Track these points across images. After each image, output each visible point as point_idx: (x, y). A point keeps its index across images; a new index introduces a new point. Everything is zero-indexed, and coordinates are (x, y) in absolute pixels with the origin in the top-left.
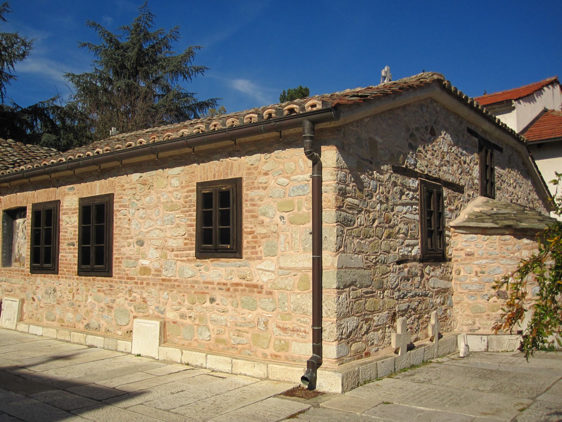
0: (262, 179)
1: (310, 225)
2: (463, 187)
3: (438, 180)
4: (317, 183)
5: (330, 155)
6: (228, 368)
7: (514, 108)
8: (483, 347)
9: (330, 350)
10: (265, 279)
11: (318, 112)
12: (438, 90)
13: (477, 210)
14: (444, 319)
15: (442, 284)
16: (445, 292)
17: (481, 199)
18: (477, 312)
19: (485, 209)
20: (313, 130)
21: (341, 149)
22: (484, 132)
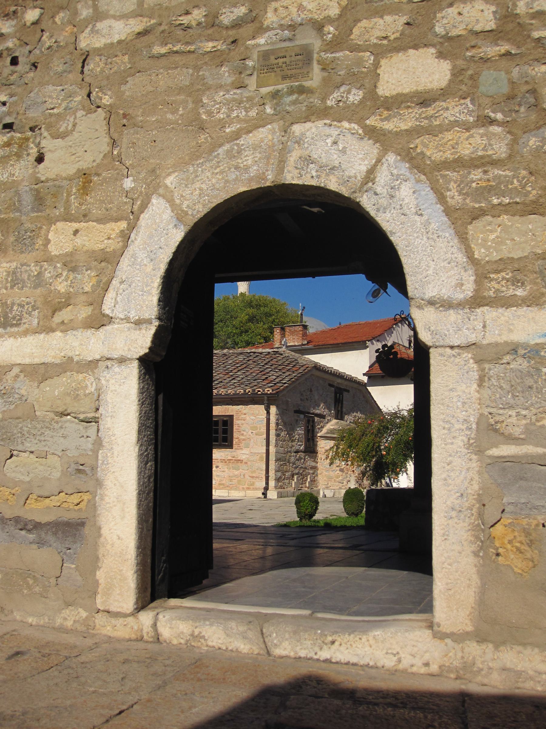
0: (243, 416)
1: (265, 436)
2: (325, 416)
3: (313, 414)
4: (268, 420)
5: (273, 409)
6: (226, 494)
7: (367, 347)
8: (332, 495)
9: (272, 483)
10: (244, 457)
11: (271, 394)
12: (314, 370)
13: (332, 427)
14: (313, 481)
15: (313, 464)
16: (315, 468)
17: (334, 421)
18: (330, 478)
19: (336, 427)
20: (268, 400)
21: (278, 407)
22: (338, 383)
